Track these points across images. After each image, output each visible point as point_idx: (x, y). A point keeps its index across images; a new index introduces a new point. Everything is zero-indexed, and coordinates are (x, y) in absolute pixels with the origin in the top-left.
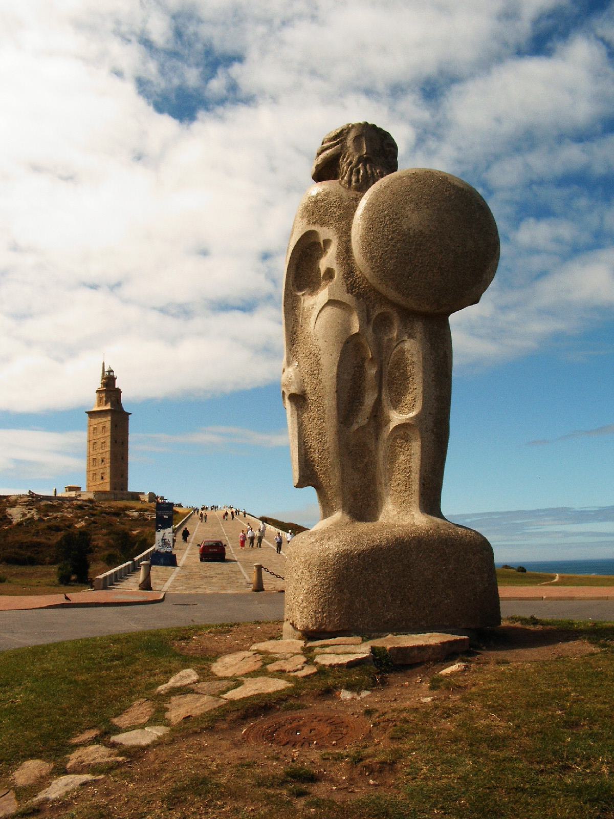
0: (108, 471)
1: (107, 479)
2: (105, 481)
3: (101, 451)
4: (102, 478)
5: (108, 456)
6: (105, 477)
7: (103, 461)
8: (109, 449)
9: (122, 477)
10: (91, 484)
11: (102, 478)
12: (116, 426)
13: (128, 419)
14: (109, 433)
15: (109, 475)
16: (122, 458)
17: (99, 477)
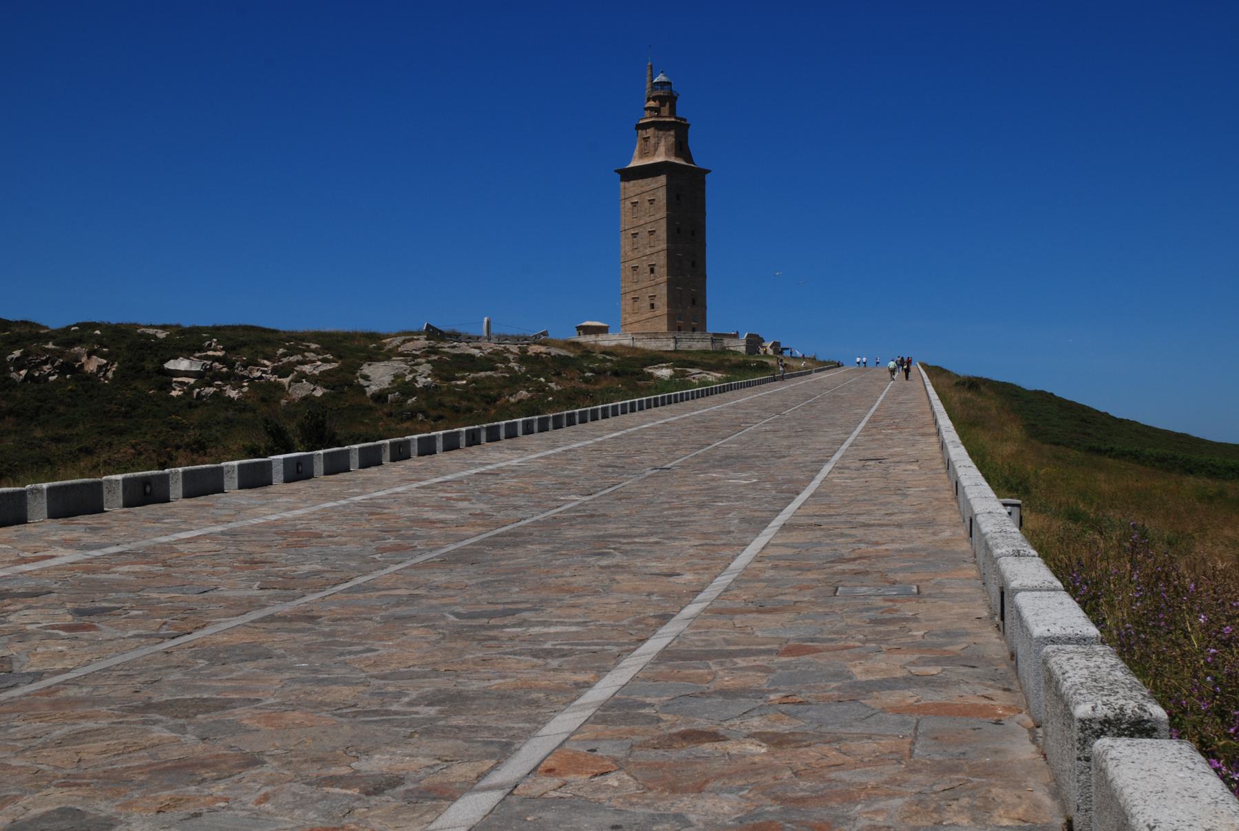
0: (663, 291)
1: (662, 308)
2: (657, 313)
3: (648, 251)
4: (652, 306)
5: (661, 261)
6: (656, 303)
7: (652, 271)
8: (664, 246)
9: (694, 303)
10: (629, 320)
11: (652, 306)
12: (678, 197)
13: (703, 182)
14: (663, 213)
15: (665, 299)
16: (693, 264)
17: (646, 304)
